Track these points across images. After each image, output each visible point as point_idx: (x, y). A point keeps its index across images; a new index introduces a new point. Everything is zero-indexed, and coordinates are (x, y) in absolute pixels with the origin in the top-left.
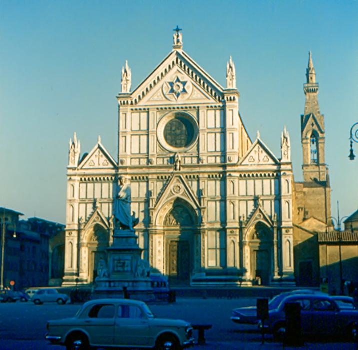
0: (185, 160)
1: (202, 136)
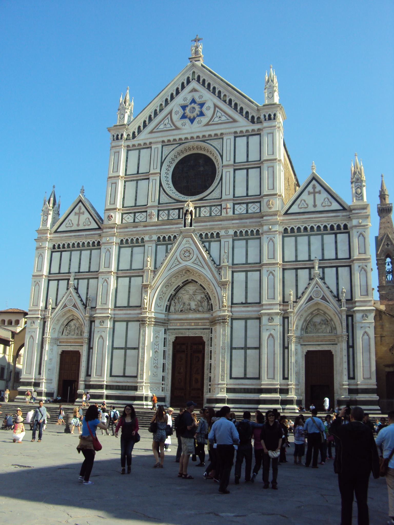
0: (200, 210)
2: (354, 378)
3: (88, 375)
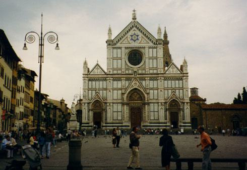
1: (147, 61)
2: (184, 119)
3: (106, 120)
